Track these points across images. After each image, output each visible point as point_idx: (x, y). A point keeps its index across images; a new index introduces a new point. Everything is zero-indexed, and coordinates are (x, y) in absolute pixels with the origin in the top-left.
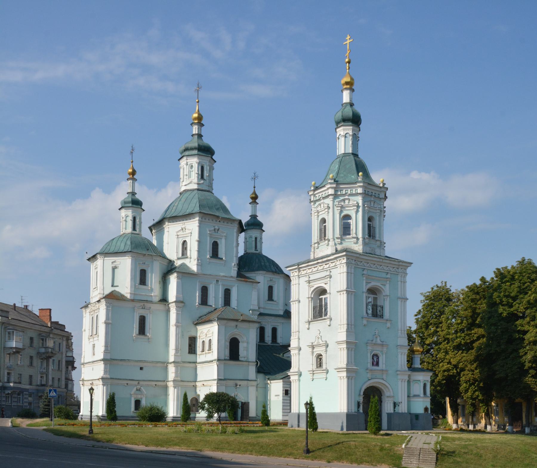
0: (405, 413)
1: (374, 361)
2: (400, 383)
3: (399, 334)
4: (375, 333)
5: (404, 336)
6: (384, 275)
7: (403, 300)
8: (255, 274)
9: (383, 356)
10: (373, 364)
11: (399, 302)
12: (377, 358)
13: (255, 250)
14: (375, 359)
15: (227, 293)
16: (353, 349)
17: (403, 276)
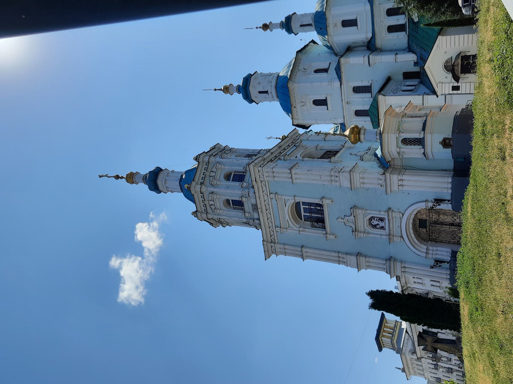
0: (452, 183)
1: (378, 224)
2: (405, 188)
3: (338, 184)
4: (342, 222)
5: (337, 179)
6: (274, 201)
7: (294, 176)
8: (333, 44)
9: (370, 214)
10: (382, 228)
11: (298, 181)
12: (374, 220)
13: (312, 26)
14: (375, 222)
15: (357, 90)
16: (367, 260)
17: (267, 174)
